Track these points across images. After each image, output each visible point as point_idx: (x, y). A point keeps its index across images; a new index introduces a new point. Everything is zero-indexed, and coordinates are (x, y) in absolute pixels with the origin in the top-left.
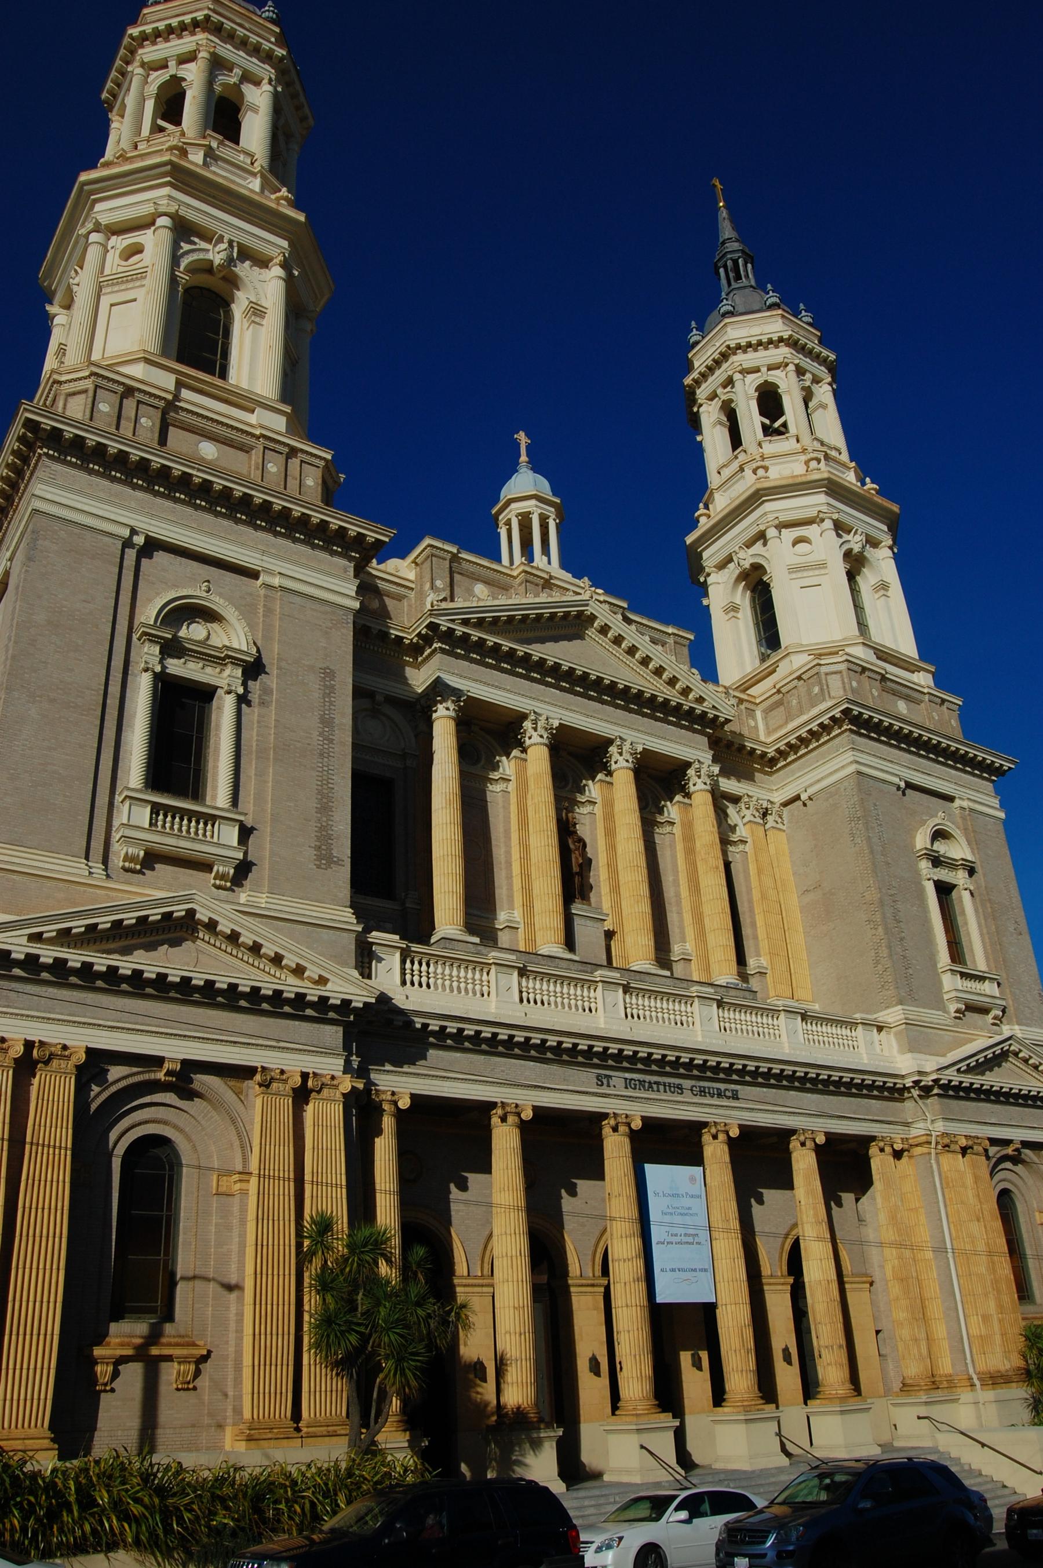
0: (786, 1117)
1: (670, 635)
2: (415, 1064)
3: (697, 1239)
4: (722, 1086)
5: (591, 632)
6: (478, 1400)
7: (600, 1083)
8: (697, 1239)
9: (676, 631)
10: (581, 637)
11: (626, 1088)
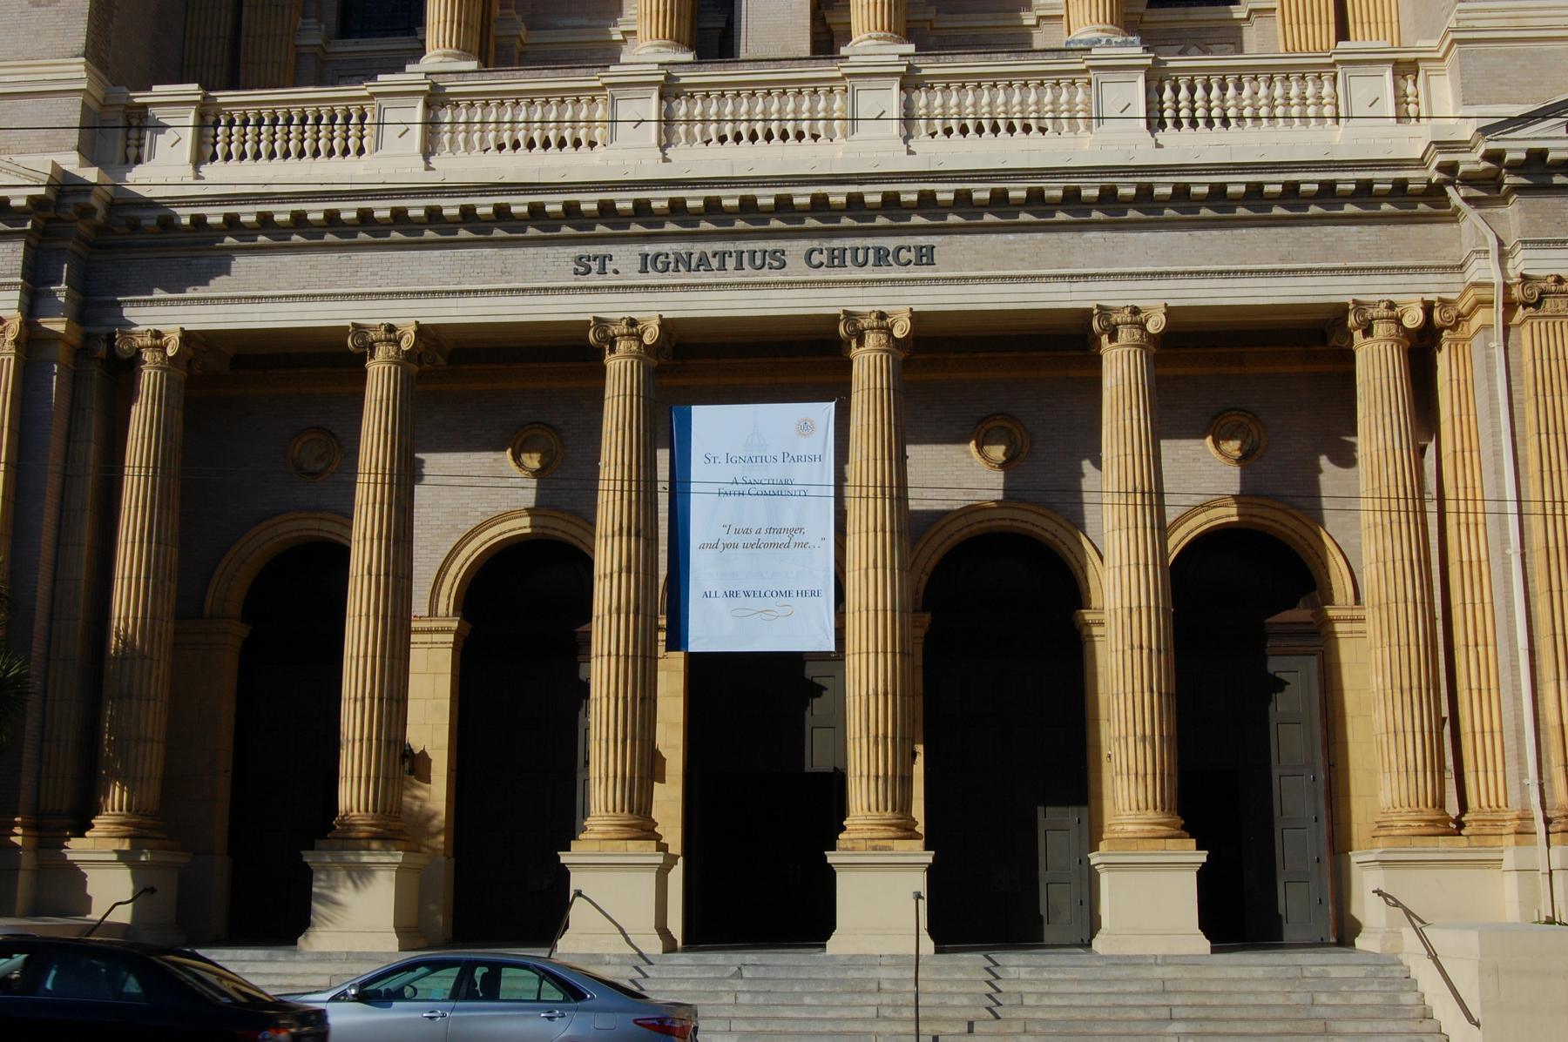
0: (1064, 286)
2: (207, 284)
3: (798, 538)
4: (890, 243)
6: (416, 808)
7: (581, 269)
8: (798, 538)
11: (644, 270)
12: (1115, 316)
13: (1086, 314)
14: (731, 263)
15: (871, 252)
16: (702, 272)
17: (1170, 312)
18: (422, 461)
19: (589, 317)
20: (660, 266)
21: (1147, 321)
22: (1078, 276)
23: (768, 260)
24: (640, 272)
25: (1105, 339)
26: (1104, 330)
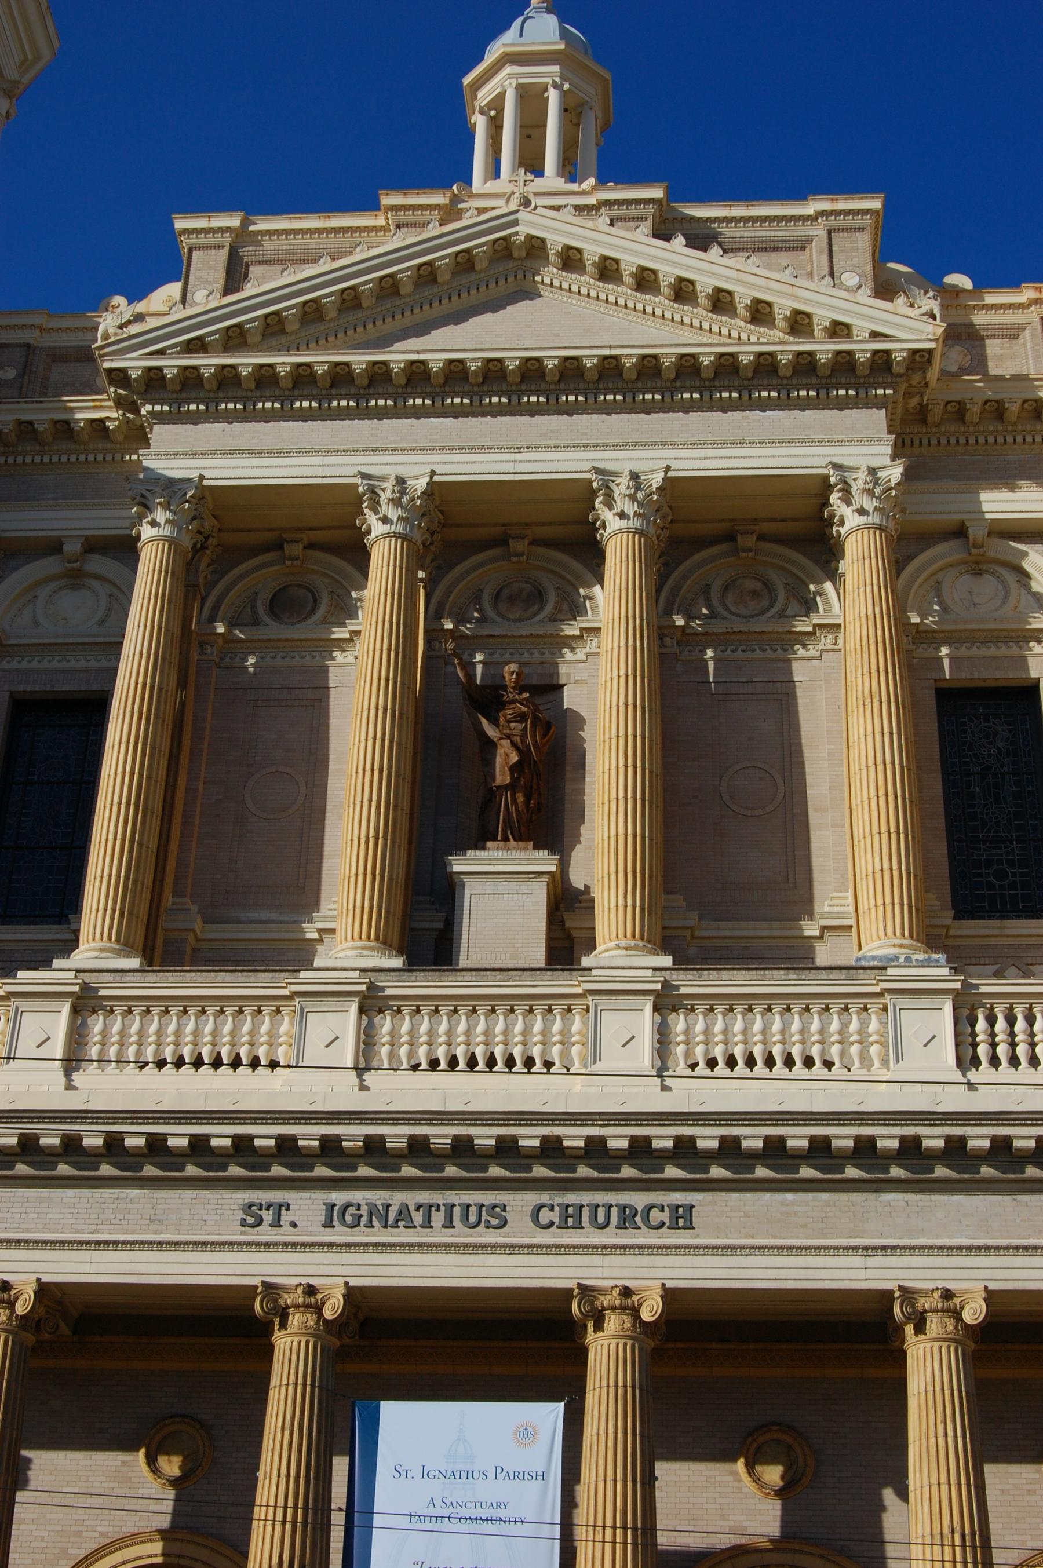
0: (856, 1261)
1: (813, 218)
4: (638, 1200)
5: (550, 274)
7: (250, 1220)
9: (825, 205)
10: (532, 294)
11: (329, 1224)
12: (922, 1301)
13: (887, 1296)
14: (438, 1218)
15: (614, 1211)
16: (402, 1229)
17: (991, 1297)
18: (28, 1461)
19: (256, 1281)
20: (349, 1219)
21: (962, 1308)
22: (875, 1248)
23: (485, 1216)
24: (324, 1226)
25: (909, 1330)
26: (908, 1319)
